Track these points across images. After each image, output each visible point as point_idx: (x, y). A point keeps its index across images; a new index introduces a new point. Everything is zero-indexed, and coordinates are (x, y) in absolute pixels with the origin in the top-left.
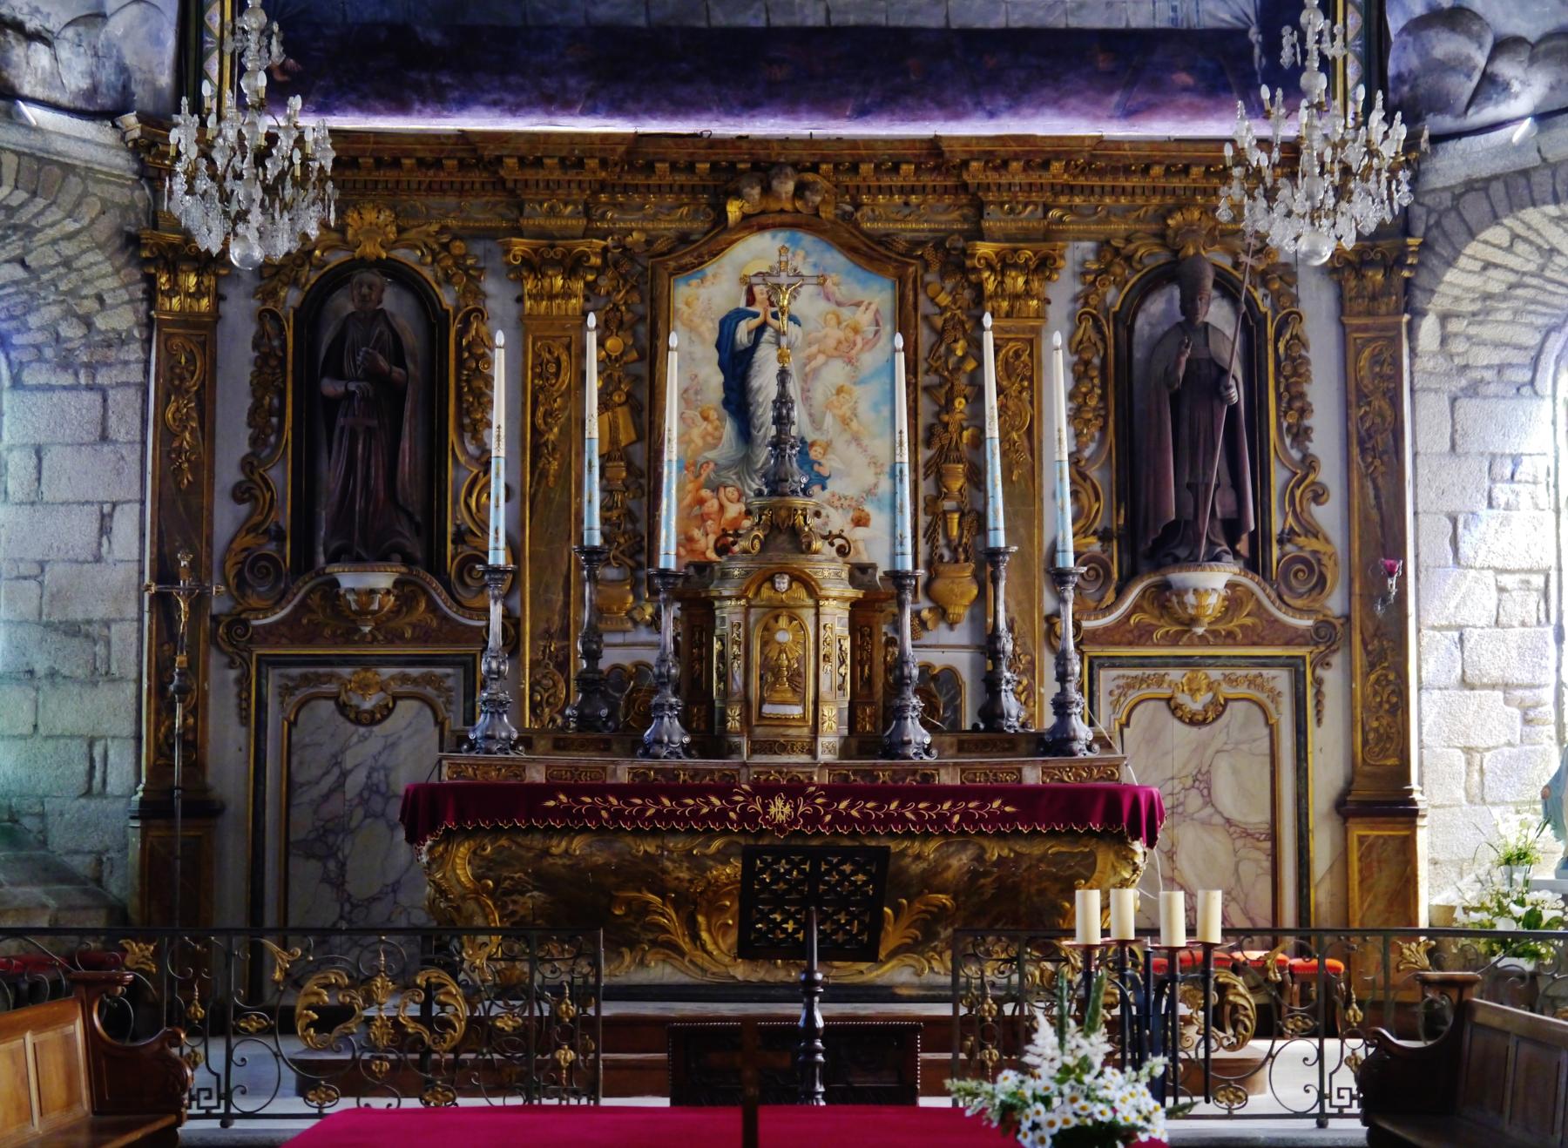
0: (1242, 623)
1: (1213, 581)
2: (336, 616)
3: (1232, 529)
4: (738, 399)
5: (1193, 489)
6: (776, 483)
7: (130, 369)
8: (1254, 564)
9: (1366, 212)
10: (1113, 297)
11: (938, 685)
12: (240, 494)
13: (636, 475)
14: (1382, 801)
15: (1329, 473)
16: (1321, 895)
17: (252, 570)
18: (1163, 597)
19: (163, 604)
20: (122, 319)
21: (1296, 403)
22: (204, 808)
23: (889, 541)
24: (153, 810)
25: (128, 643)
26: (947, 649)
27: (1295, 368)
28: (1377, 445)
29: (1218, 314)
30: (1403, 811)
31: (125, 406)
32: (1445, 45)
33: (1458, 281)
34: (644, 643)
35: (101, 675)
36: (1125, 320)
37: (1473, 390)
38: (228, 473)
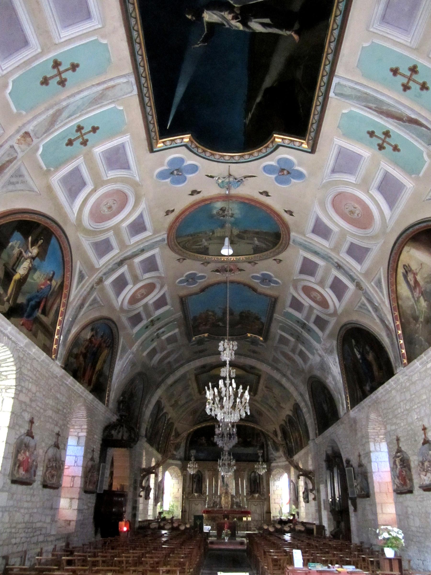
0: (259, 498)
1: (257, 495)
2: (194, 497)
3: (258, 491)
4: (223, 481)
5: (255, 488)
6: (227, 489)
7: (181, 478)
8: (260, 494)
9: (264, 471)
10: (250, 473)
11: (237, 503)
12: (189, 487)
13: (217, 486)
14: (269, 512)
15: (265, 487)
16: (265, 519)
17: (189, 493)
18: (253, 496)
19: (183, 496)
20: (180, 474)
21: (263, 482)
22: (185, 511)
23: (233, 492)
24: (182, 511)
25: (180, 499)
26: (238, 500)
27: (262, 479)
28: (268, 485)
29: (257, 475)
30: (270, 513)
31: (180, 481)
32: (272, 456)
33: (273, 473)
34: (218, 500)
35: (178, 501)
36: (250, 475)
37: (275, 481)
38: (187, 486)
